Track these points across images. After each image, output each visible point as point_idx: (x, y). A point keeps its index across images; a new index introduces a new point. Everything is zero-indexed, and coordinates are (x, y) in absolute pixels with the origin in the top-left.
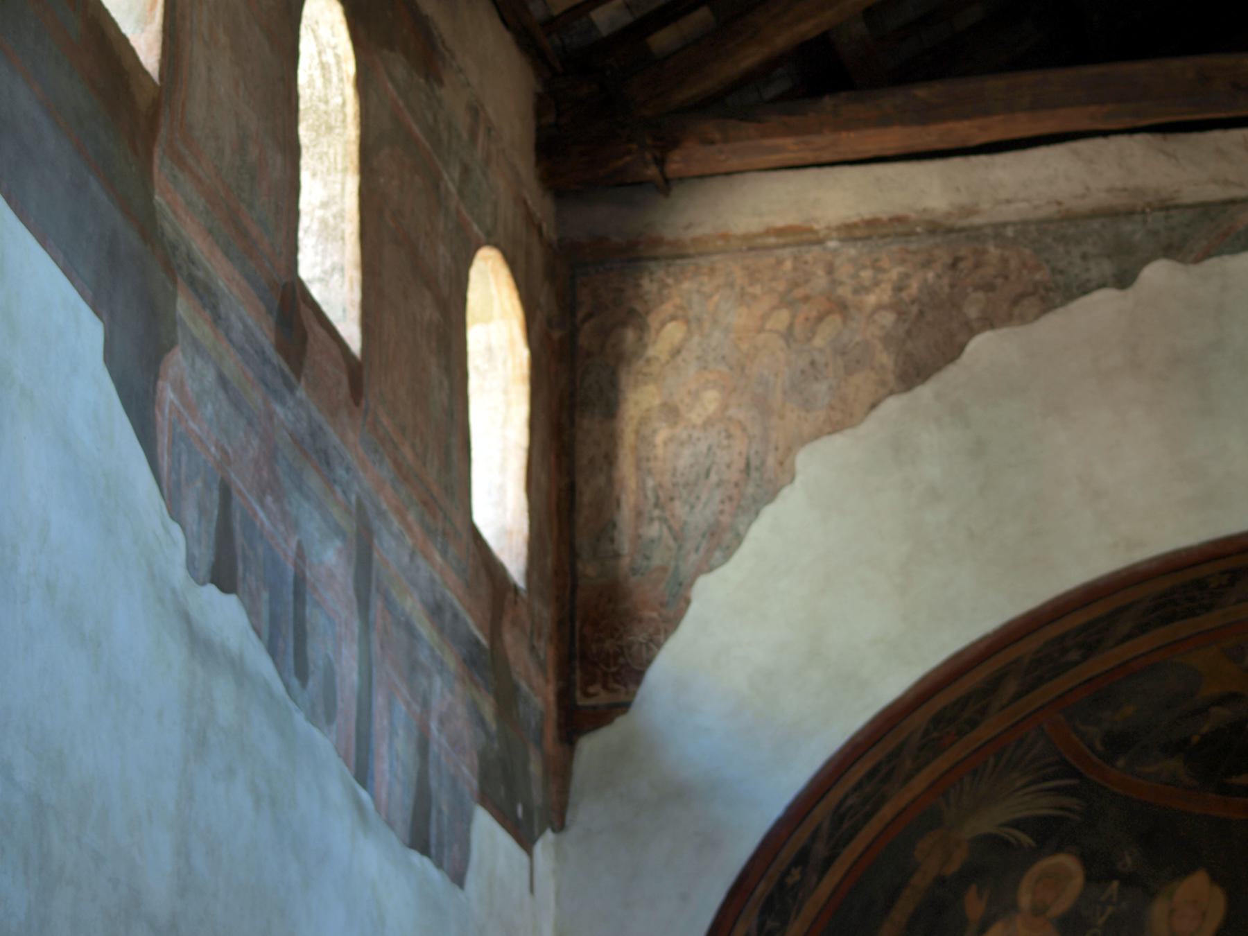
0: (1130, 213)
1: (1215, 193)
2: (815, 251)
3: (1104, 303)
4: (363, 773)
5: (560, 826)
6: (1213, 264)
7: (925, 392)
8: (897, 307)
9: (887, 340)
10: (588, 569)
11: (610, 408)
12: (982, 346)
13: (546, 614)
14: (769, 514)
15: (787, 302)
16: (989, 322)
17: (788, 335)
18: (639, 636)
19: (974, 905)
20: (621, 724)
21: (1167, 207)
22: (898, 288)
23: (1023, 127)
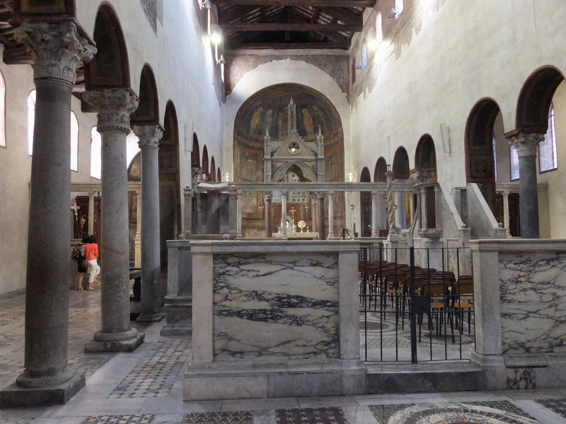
0: (271, 56)
1: (278, 55)
2: (246, 57)
3: (269, 63)
4: (218, 100)
5: (225, 103)
6: (278, 61)
7: (255, 69)
8: (253, 62)
9: (252, 65)
10: (227, 82)
11: (229, 68)
12: (259, 66)
13: (224, 85)
14: (242, 78)
15: (244, 60)
16: (260, 64)
17: (244, 63)
18: (231, 88)
19: (255, 111)
20: (230, 95)
21: (275, 55)
22: (253, 60)
23: (264, 48)
